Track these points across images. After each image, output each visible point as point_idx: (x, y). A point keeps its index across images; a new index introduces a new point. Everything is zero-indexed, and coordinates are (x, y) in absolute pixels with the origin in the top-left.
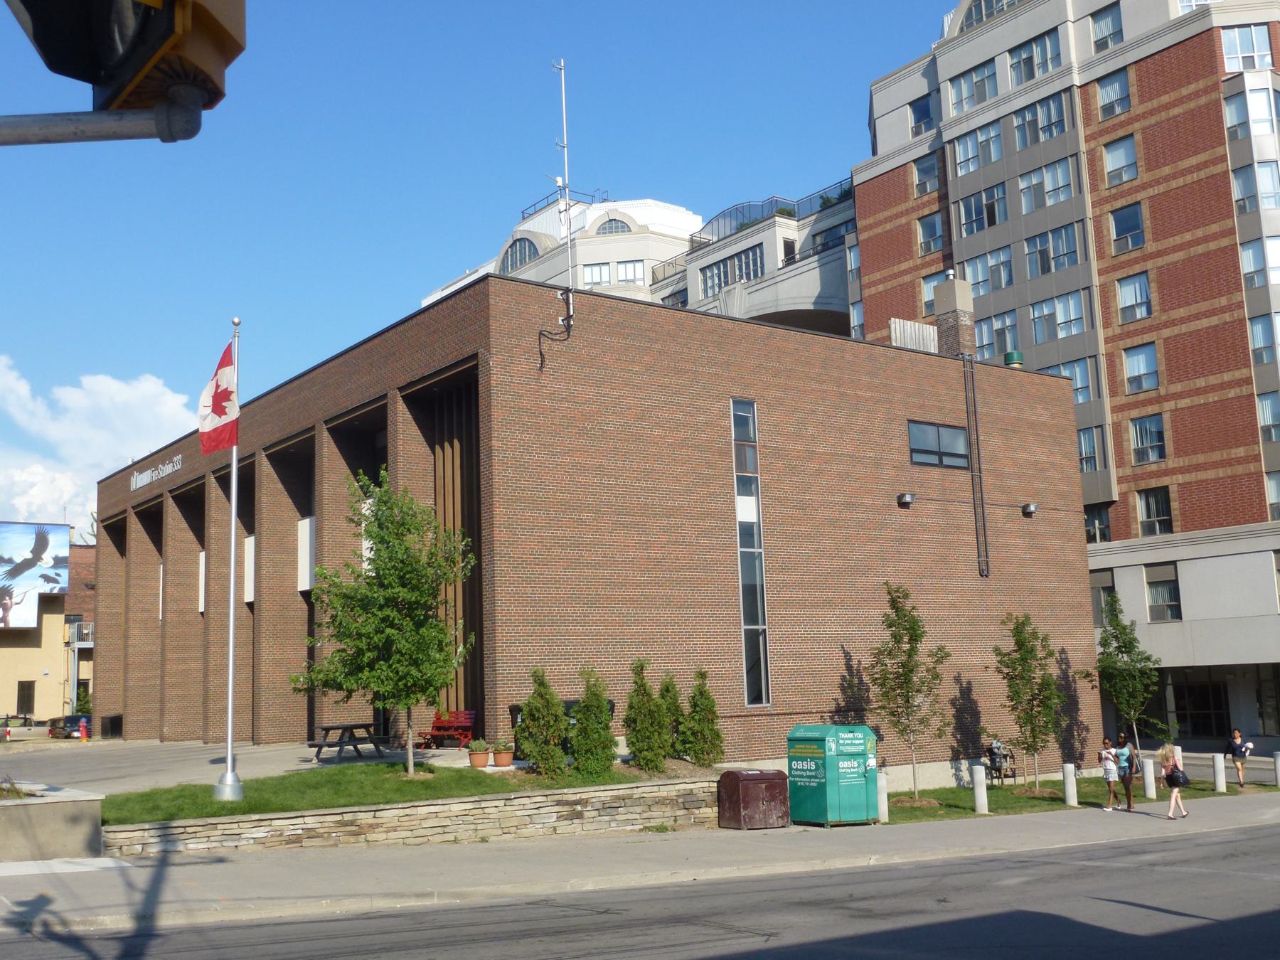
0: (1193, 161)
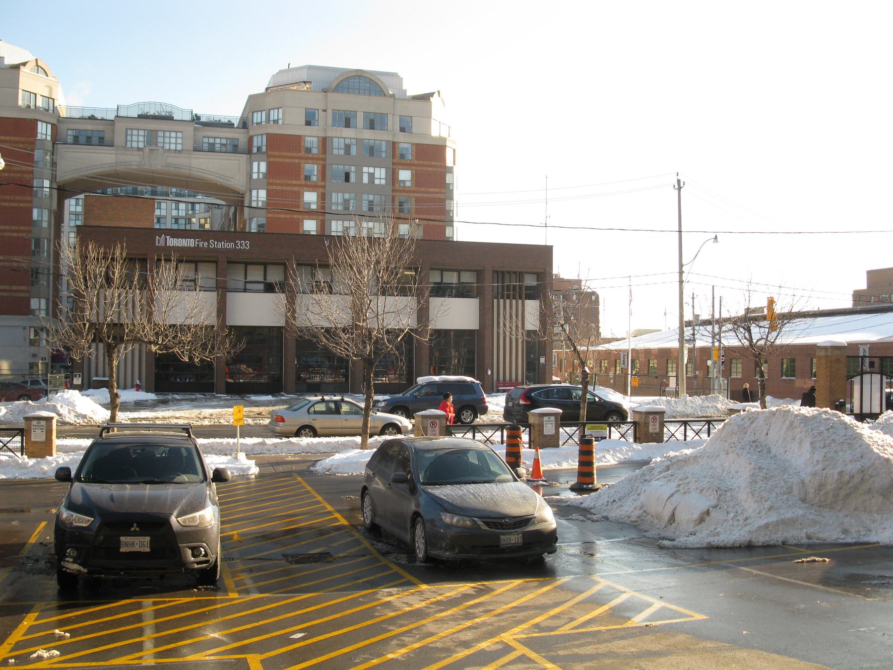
0: (434, 190)
